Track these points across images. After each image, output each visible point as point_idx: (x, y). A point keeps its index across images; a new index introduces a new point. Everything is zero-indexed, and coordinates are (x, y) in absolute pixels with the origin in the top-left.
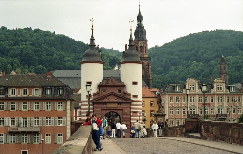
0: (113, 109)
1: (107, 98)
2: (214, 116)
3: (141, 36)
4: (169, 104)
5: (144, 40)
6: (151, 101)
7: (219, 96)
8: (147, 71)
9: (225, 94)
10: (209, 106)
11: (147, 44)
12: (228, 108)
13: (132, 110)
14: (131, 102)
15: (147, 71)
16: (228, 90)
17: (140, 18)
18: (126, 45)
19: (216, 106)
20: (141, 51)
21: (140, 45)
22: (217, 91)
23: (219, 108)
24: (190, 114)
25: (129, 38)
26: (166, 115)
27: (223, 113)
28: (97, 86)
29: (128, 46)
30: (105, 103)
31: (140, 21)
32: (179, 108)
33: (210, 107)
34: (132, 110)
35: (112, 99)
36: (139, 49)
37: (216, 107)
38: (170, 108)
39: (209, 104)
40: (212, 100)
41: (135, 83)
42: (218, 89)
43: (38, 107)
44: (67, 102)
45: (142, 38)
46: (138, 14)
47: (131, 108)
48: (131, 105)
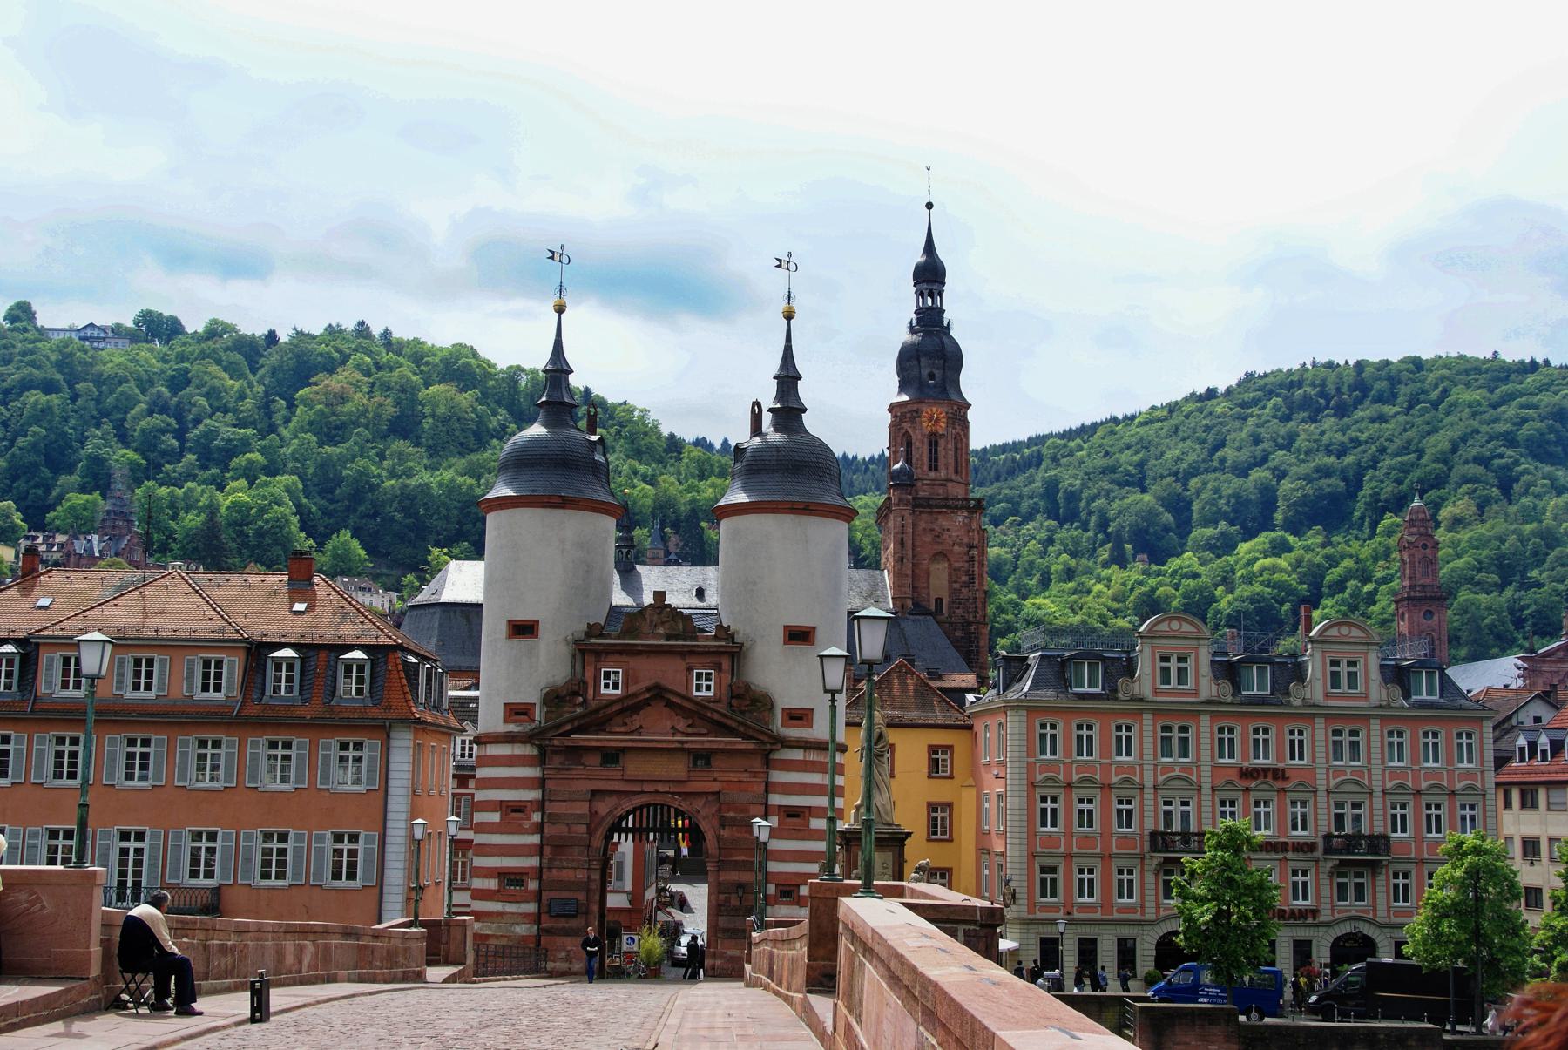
0: (661, 788)
2: (1311, 847)
4: (1030, 767)
5: (950, 402)
6: (933, 749)
8: (965, 578)
9: (1377, 716)
10: (1278, 785)
11: (965, 425)
13: (776, 799)
14: (771, 750)
15: (965, 578)
16: (1398, 691)
17: (930, 275)
18: (757, 404)
19: (1321, 785)
20: (934, 465)
21: (926, 426)
22: (1326, 696)
23: (1339, 798)
24: (1161, 828)
25: (774, 365)
26: (909, 835)
28: (564, 651)
29: (770, 410)
30: (611, 756)
31: (931, 295)
32: (1129, 793)
33: (1283, 790)
34: (776, 799)
35: (659, 728)
36: (921, 451)
37: (1322, 795)
38: (1039, 792)
39: (1278, 774)
40: (1296, 750)
41: (799, 636)
42: (1335, 683)
43: (144, 767)
44: (394, 743)
45: (935, 386)
46: (918, 257)
47: (769, 787)
48: (768, 764)
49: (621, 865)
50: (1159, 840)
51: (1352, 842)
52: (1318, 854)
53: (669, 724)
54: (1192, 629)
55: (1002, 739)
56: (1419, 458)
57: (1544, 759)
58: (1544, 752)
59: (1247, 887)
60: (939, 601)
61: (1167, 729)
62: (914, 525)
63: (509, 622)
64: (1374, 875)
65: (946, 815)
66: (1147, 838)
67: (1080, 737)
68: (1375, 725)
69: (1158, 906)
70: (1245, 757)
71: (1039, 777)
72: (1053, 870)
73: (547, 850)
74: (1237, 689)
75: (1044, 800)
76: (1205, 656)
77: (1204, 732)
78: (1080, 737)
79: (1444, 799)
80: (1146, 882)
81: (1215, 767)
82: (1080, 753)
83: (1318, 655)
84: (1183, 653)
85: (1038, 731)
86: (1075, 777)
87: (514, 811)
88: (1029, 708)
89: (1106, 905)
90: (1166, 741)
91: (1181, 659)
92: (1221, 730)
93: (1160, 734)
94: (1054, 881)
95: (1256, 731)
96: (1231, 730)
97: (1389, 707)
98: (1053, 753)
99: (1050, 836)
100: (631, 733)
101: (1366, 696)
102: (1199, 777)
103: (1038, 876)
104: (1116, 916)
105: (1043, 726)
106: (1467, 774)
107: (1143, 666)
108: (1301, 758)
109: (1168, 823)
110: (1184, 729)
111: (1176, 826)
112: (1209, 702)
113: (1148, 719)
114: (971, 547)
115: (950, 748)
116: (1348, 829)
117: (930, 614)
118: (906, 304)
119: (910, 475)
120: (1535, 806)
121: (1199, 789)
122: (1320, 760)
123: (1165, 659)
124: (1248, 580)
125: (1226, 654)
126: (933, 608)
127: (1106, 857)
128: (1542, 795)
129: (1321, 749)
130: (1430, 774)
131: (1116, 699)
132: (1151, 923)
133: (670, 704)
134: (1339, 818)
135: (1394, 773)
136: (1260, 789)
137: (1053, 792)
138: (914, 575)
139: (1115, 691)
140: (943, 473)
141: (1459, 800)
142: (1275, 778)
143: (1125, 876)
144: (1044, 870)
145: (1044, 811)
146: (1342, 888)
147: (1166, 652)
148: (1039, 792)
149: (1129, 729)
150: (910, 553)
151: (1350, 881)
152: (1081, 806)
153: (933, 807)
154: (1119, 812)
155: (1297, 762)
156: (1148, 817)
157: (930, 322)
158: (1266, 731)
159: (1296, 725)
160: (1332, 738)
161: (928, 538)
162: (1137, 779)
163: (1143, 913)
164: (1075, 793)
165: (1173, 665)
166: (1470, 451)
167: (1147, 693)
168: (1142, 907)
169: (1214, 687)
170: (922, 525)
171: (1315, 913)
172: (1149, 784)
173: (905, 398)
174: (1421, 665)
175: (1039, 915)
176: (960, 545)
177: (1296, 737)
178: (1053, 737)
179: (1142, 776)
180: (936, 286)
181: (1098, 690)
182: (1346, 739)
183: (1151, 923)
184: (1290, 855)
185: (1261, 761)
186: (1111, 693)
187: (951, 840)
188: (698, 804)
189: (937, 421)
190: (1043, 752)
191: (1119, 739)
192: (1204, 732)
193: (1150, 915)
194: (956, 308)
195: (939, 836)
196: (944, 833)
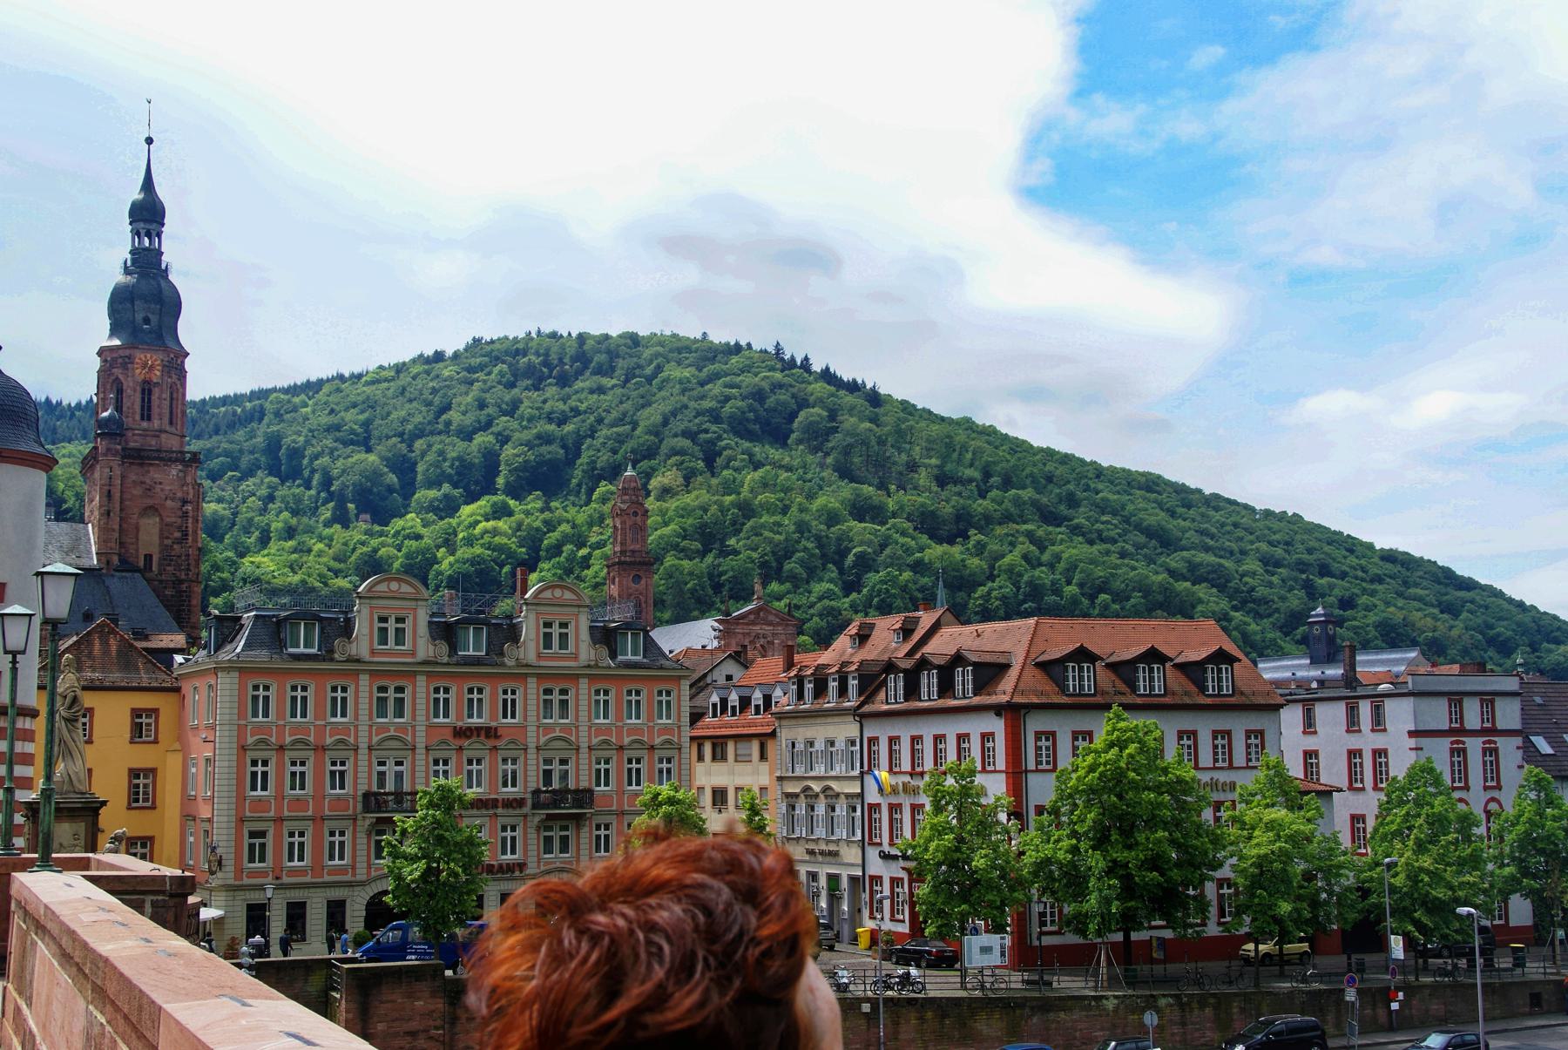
2: (520, 803)
3: (147, 321)
4: (241, 729)
5: (166, 349)
6: (136, 713)
7: (548, 686)
8: (178, 535)
10: (490, 743)
11: (182, 374)
12: (600, 754)
15: (178, 535)
16: (605, 652)
17: (148, 214)
19: (532, 742)
20: (146, 415)
21: (139, 374)
22: (539, 656)
23: (549, 754)
24: (375, 789)
26: (104, 803)
27: (571, 786)
31: (149, 235)
36: (133, 400)
38: (250, 755)
39: (490, 732)
40: (508, 709)
46: (136, 194)
50: (372, 801)
51: (559, 797)
52: (527, 810)
54: (410, 589)
55: (212, 703)
56: (634, 429)
57: (734, 714)
58: (734, 708)
59: (456, 844)
60: (148, 558)
61: (383, 689)
62: (123, 477)
64: (578, 828)
65: (149, 781)
66: (360, 799)
67: (294, 699)
68: (584, 684)
69: (369, 867)
70: (459, 717)
71: (250, 740)
72: (262, 834)
74: (453, 649)
75: (254, 763)
76: (423, 617)
77: (420, 693)
78: (294, 699)
79: (644, 754)
80: (357, 843)
81: (430, 727)
82: (294, 715)
83: (532, 616)
84: (401, 614)
85: (251, 692)
86: (288, 739)
88: (241, 669)
89: (317, 867)
90: (382, 702)
91: (400, 620)
92: (437, 690)
93: (376, 694)
94: (263, 846)
95: (471, 691)
96: (446, 690)
97: (597, 666)
98: (266, 715)
99: (260, 800)
101: (576, 657)
102: (414, 736)
103: (246, 841)
104: (327, 878)
105: (256, 688)
106: (666, 730)
107: (361, 626)
108: (513, 716)
109: (382, 783)
110: (400, 689)
111: (390, 786)
112: (425, 663)
113: (364, 680)
114: (185, 502)
115: (156, 711)
116: (556, 785)
117: (138, 570)
118: (118, 246)
119: (120, 424)
120: (724, 758)
121: (414, 749)
122: (532, 719)
123: (383, 619)
124: (469, 542)
125: (444, 615)
126: (141, 564)
127: (318, 820)
128: (731, 747)
129: (532, 708)
130: (633, 730)
131: (332, 660)
132: (362, 884)
134: (548, 775)
135: (600, 730)
136: (474, 748)
137: (265, 755)
138: (121, 530)
139: (332, 651)
140: (156, 424)
141: (657, 754)
142: (488, 737)
143: (337, 838)
144: (253, 835)
145: (254, 774)
146: (548, 840)
147: (384, 613)
148: (250, 755)
149: (344, 690)
150: (117, 506)
151: (556, 834)
152: (294, 769)
153: (134, 773)
154: (333, 773)
155: (509, 720)
156: (361, 777)
157: (147, 264)
158: (480, 691)
159: (509, 685)
160: (543, 697)
161: (137, 491)
162: (352, 740)
163: (354, 874)
164: (288, 756)
165: (391, 626)
166: (678, 425)
167: (364, 653)
168: (354, 868)
169: (431, 648)
170: (133, 477)
171: (522, 866)
172: (363, 745)
173: (117, 342)
174: (627, 626)
175: (246, 881)
176: (173, 499)
177: (509, 697)
178: (266, 699)
179: (356, 737)
180: (153, 226)
181: (314, 651)
182: (556, 697)
183: (362, 884)
184: (500, 811)
185: (475, 720)
186: (327, 654)
187: (153, 807)
189: (152, 368)
190: (255, 715)
191: (334, 700)
192: (420, 693)
193: (361, 874)
194: (175, 251)
195: (141, 804)
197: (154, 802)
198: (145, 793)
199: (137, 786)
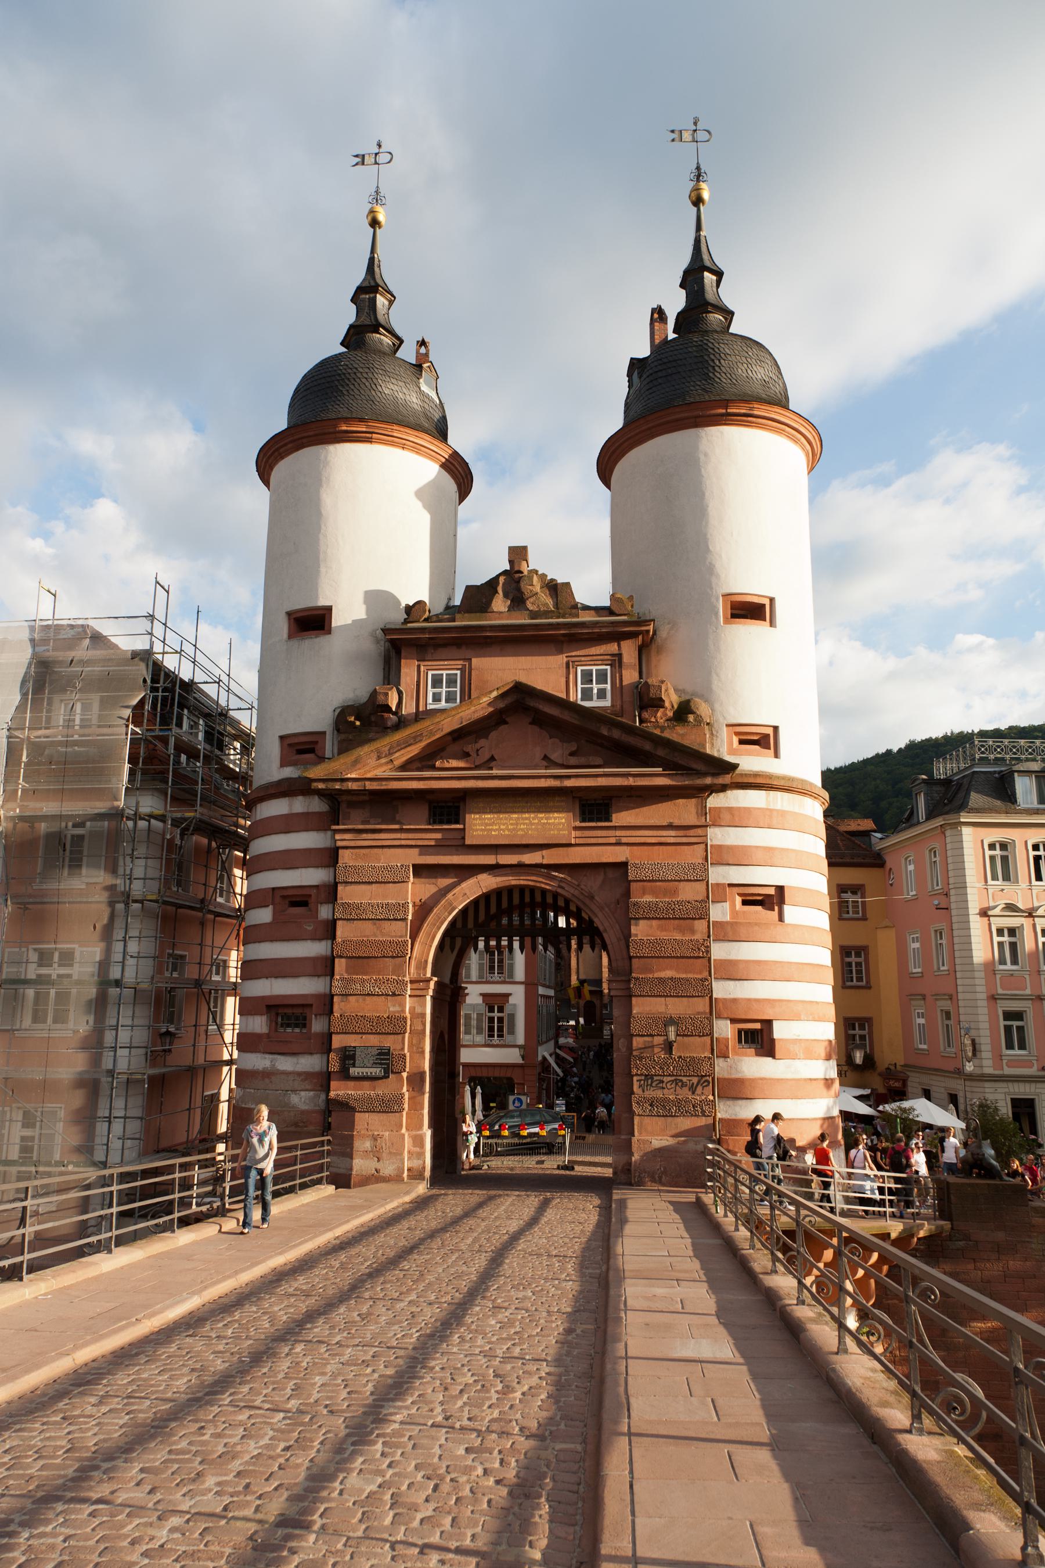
0: (529, 858)
1: (469, 748)
30: (447, 808)
41: (750, 611)
49: (512, 1017)
53: (538, 753)
63: (289, 614)
65: (861, 959)
72: (1018, 1016)
73: (340, 965)
87: (294, 904)
94: (1020, 1029)
100: (477, 768)
133: (540, 720)
144: (1008, 1016)
175: (1007, 1071)
188: (592, 883)
196: (860, 979)
197: (868, 982)
198: (859, 972)
199: (850, 964)
